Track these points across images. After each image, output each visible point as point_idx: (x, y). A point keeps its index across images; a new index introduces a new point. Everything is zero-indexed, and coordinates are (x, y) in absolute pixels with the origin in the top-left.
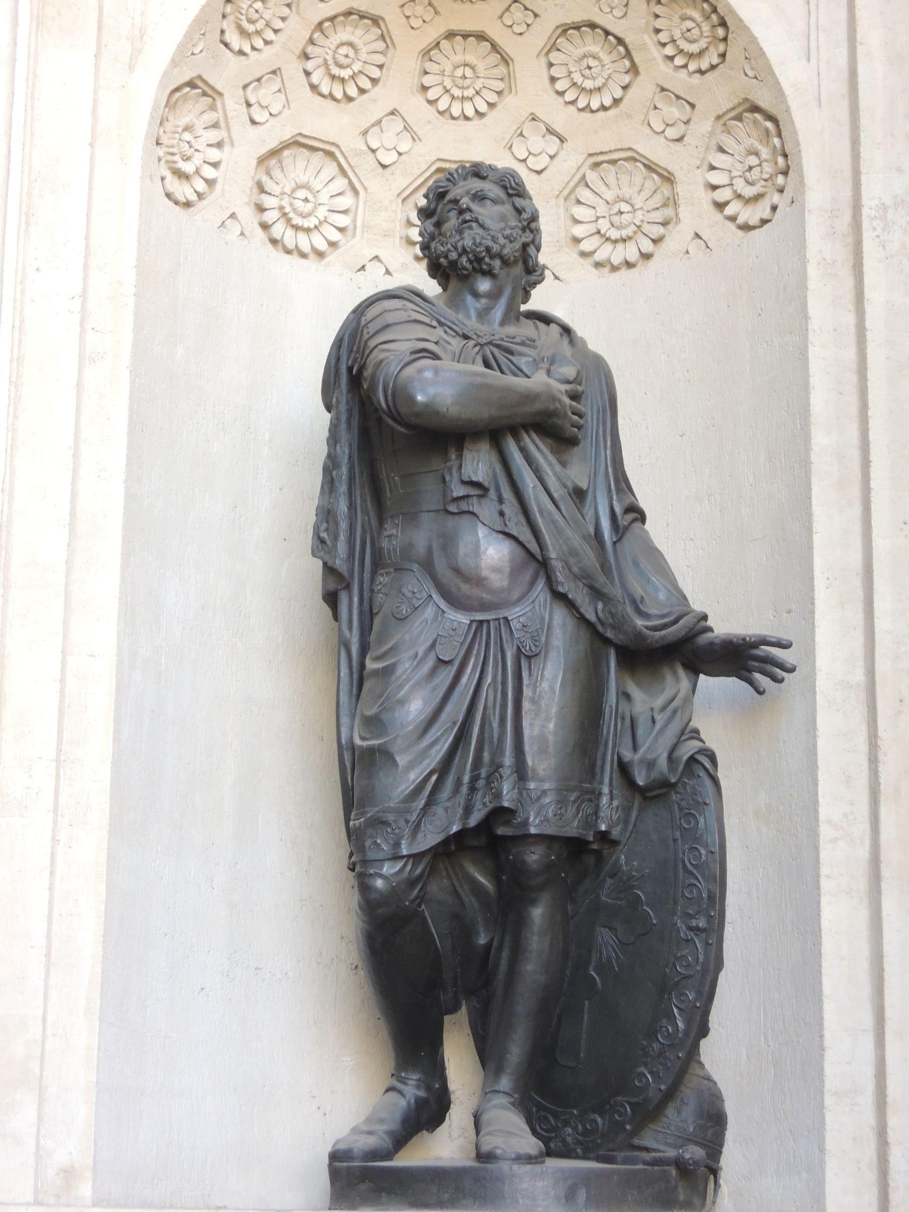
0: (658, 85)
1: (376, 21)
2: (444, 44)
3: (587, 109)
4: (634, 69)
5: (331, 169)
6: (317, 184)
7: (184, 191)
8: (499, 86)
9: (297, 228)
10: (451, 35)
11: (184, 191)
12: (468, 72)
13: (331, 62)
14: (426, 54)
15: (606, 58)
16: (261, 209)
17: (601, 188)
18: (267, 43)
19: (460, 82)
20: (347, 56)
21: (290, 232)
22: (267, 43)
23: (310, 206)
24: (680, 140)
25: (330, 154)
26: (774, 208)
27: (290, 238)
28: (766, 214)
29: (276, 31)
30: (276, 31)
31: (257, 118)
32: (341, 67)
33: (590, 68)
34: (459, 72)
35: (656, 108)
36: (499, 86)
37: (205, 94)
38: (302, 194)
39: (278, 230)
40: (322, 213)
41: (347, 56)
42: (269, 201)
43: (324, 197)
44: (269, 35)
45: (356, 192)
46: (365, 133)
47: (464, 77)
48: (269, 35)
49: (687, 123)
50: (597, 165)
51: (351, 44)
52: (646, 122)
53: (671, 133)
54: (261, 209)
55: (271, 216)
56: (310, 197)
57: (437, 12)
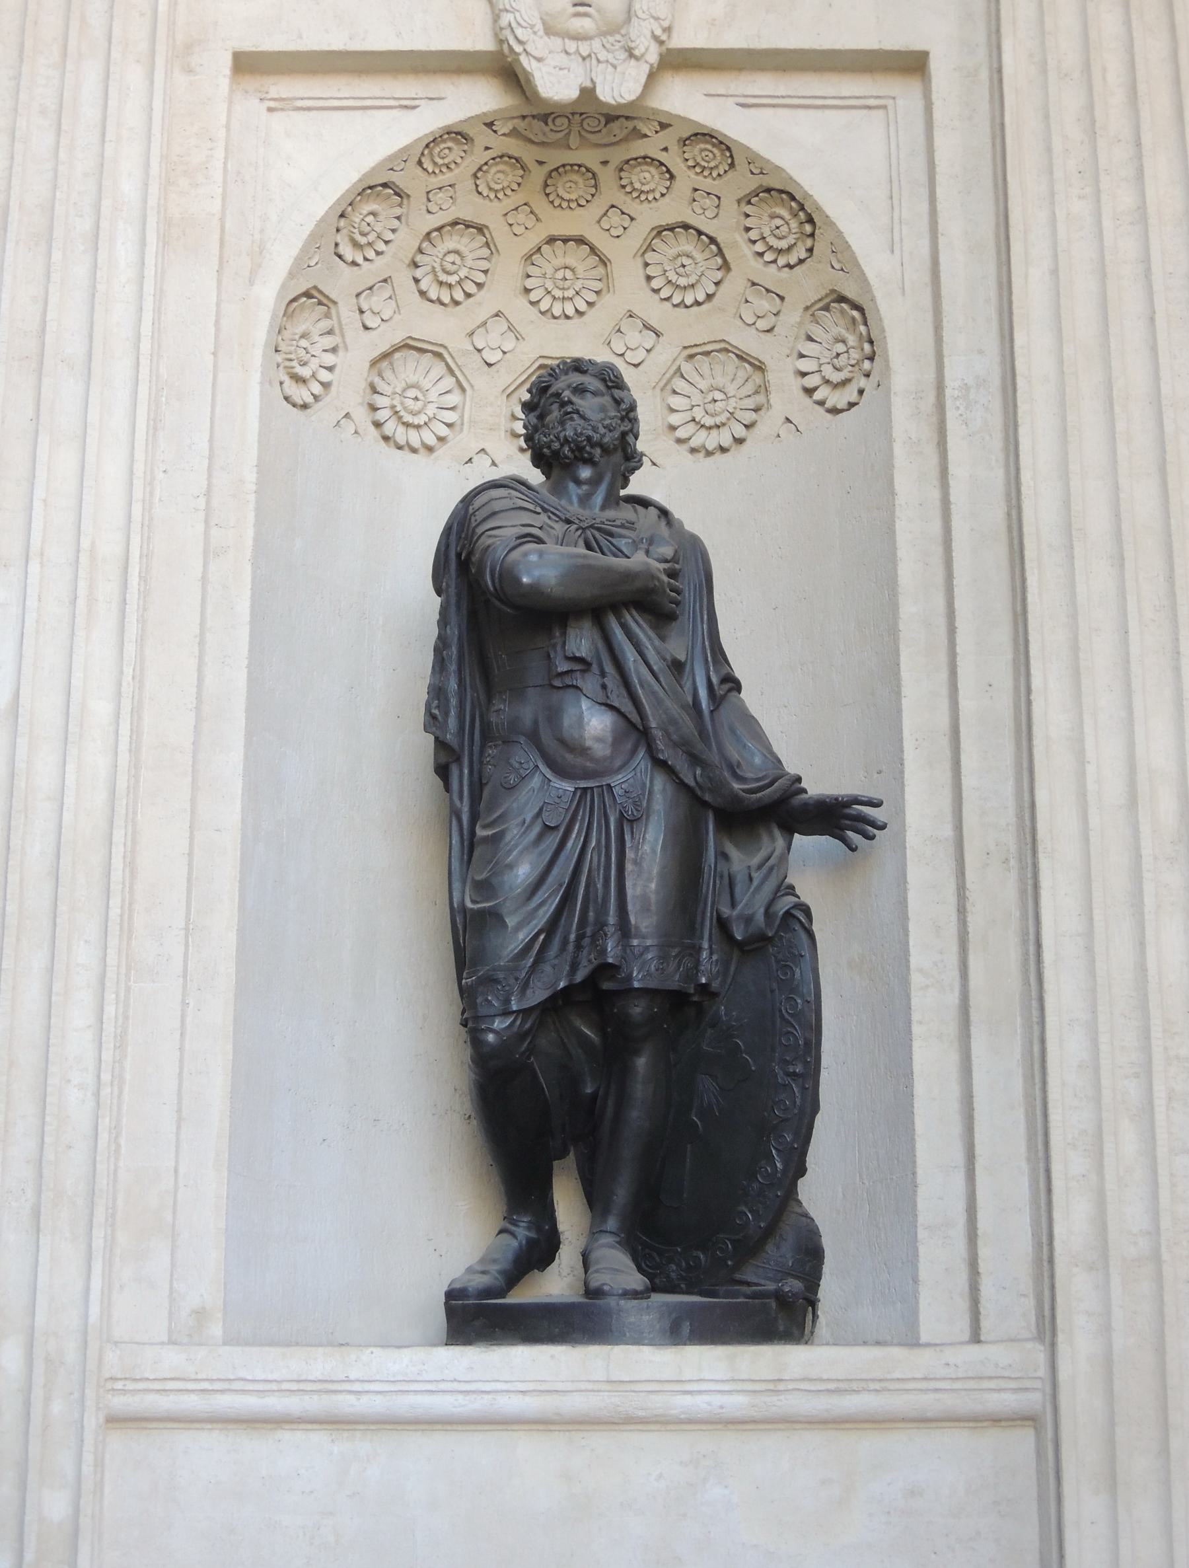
0: (749, 280)
1: (480, 229)
2: (546, 249)
3: (682, 304)
4: (726, 266)
5: (439, 369)
6: (426, 384)
7: (301, 394)
8: (597, 286)
9: (407, 425)
10: (551, 240)
11: (301, 394)
12: (569, 274)
13: (438, 269)
14: (528, 258)
15: (699, 257)
16: (374, 409)
18: (378, 253)
20: (453, 263)
21: (401, 429)
22: (378, 253)
23: (419, 404)
25: (438, 355)
26: (861, 392)
27: (401, 435)
28: (854, 397)
29: (386, 242)
30: (386, 242)
31: (369, 324)
32: (448, 273)
33: (684, 266)
34: (560, 275)
35: (747, 301)
36: (597, 286)
37: (320, 303)
38: (412, 393)
39: (389, 428)
40: (431, 410)
41: (453, 263)
42: (380, 401)
43: (433, 395)
44: (381, 246)
45: (463, 390)
46: (471, 334)
48: (381, 246)
50: (691, 357)
51: (457, 252)
52: (738, 315)
53: (762, 324)
54: (374, 409)
55: (382, 415)
56: (420, 396)
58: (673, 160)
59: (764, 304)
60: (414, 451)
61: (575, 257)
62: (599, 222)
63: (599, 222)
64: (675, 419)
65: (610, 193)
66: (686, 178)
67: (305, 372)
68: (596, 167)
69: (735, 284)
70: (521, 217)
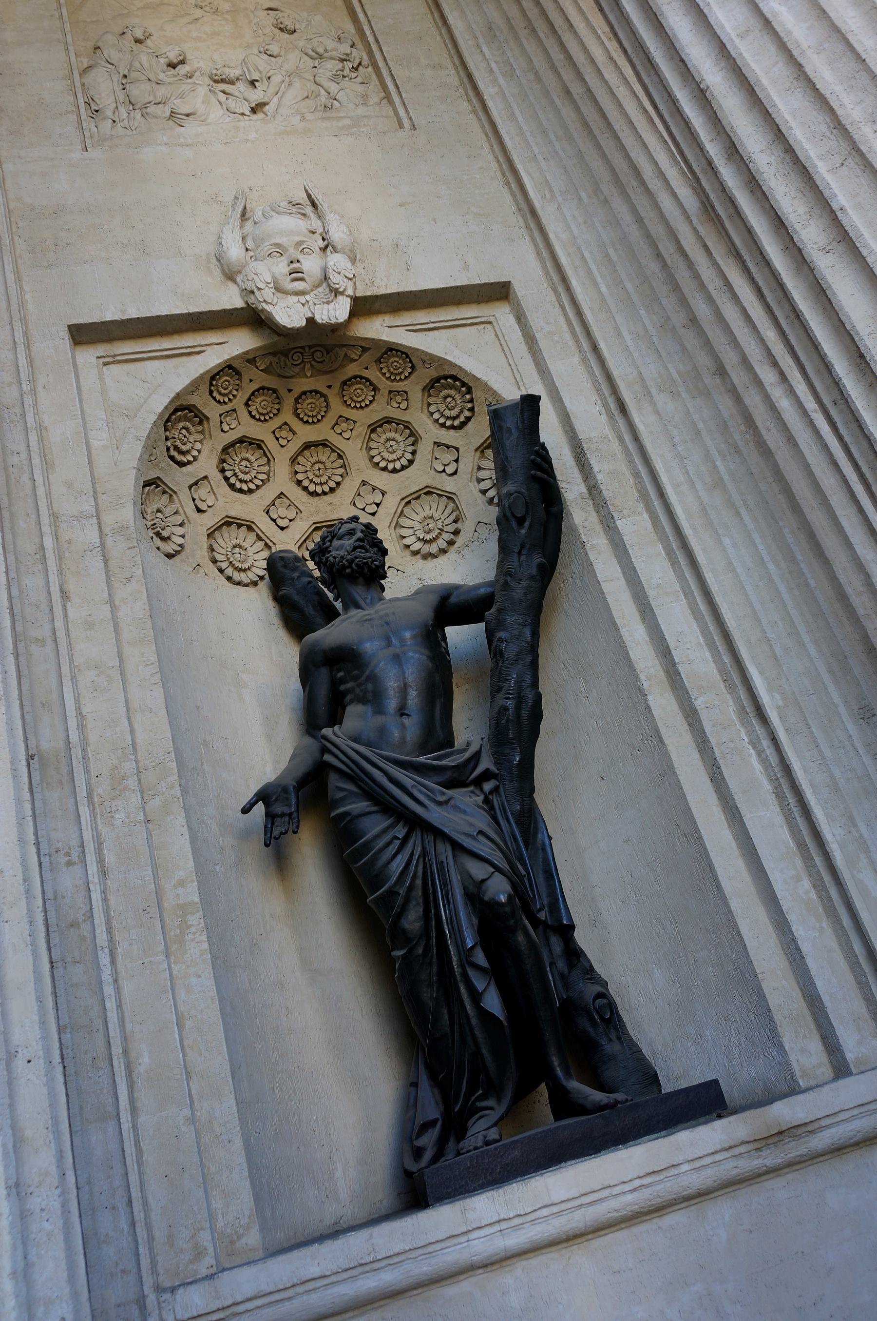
3: (395, 471)
6: (245, 544)
8: (342, 470)
10: (307, 446)
12: (321, 466)
13: (237, 471)
14: (294, 460)
15: (400, 439)
17: (414, 517)
19: (317, 472)
20: (246, 467)
24: (455, 473)
25: (250, 528)
27: (236, 576)
33: (391, 446)
35: (436, 459)
47: (319, 469)
49: (457, 461)
50: (408, 503)
52: (432, 468)
53: (450, 470)
57: (294, 433)
58: (373, 374)
59: (449, 457)
60: (247, 585)
61: (324, 455)
62: (333, 428)
63: (333, 428)
64: (407, 541)
65: (337, 408)
66: (385, 385)
67: (165, 534)
68: (325, 391)
69: (425, 448)
70: (284, 434)
